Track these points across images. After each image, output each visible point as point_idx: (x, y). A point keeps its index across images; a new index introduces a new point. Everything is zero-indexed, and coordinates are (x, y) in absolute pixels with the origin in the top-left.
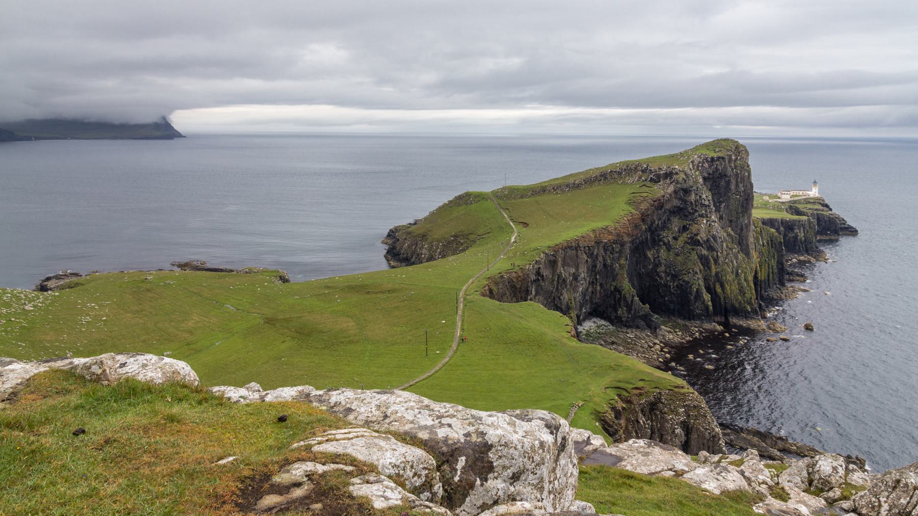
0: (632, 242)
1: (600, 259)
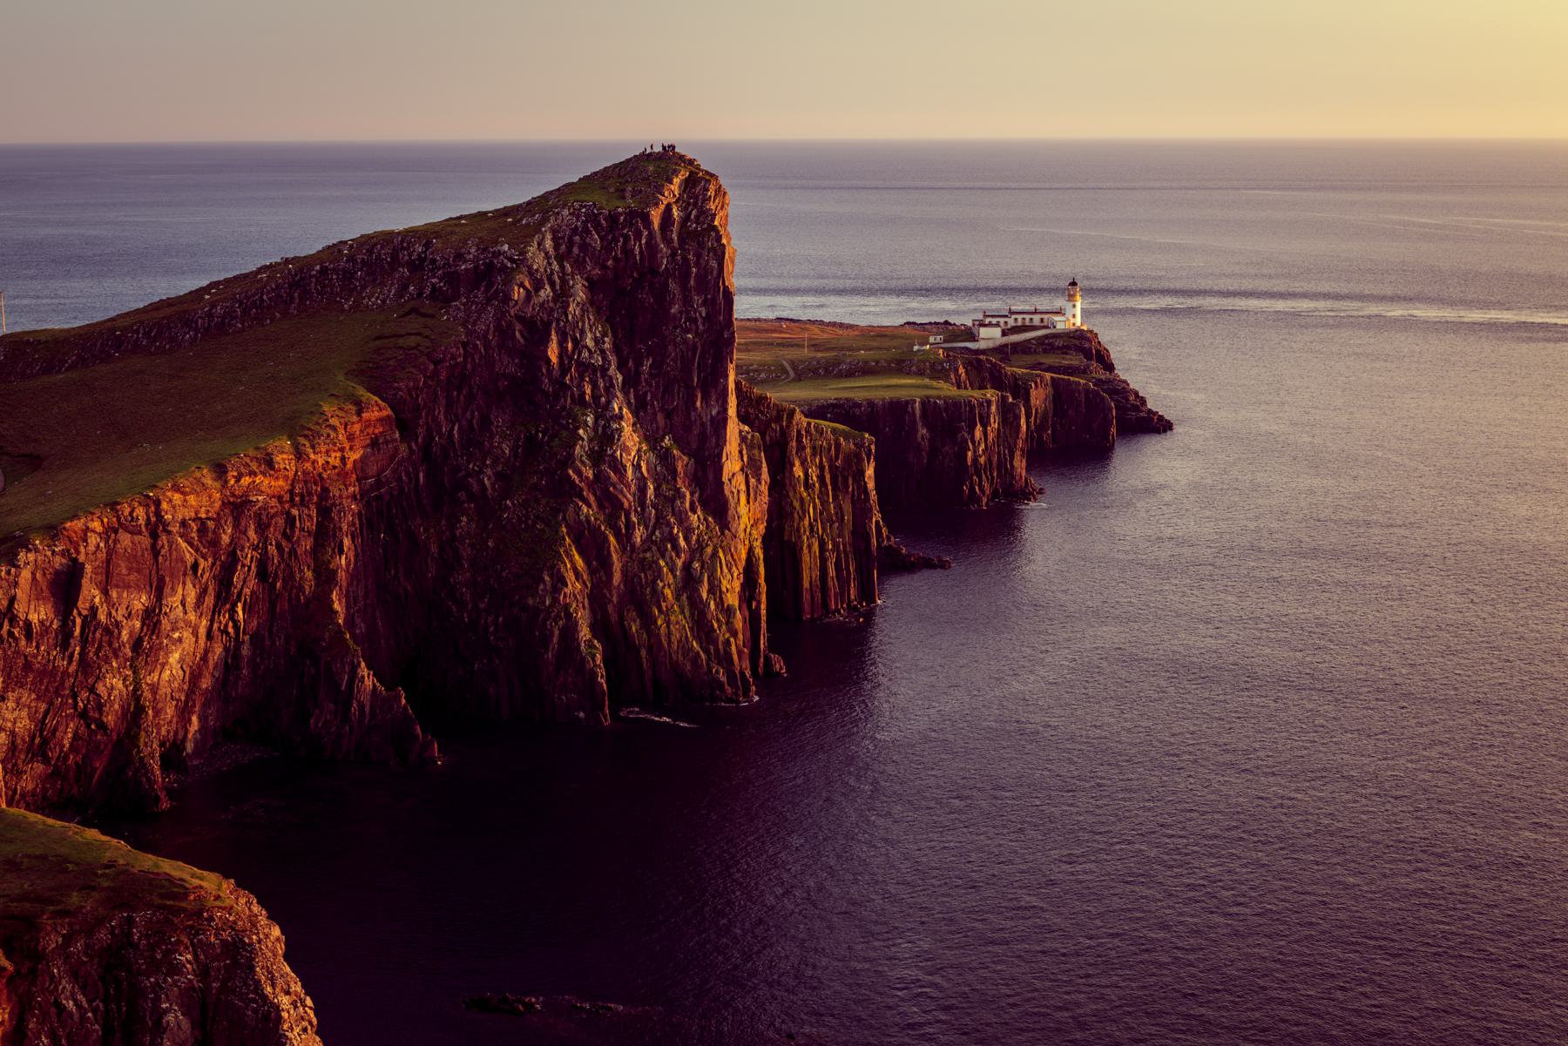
0: (363, 497)
1: (248, 556)
